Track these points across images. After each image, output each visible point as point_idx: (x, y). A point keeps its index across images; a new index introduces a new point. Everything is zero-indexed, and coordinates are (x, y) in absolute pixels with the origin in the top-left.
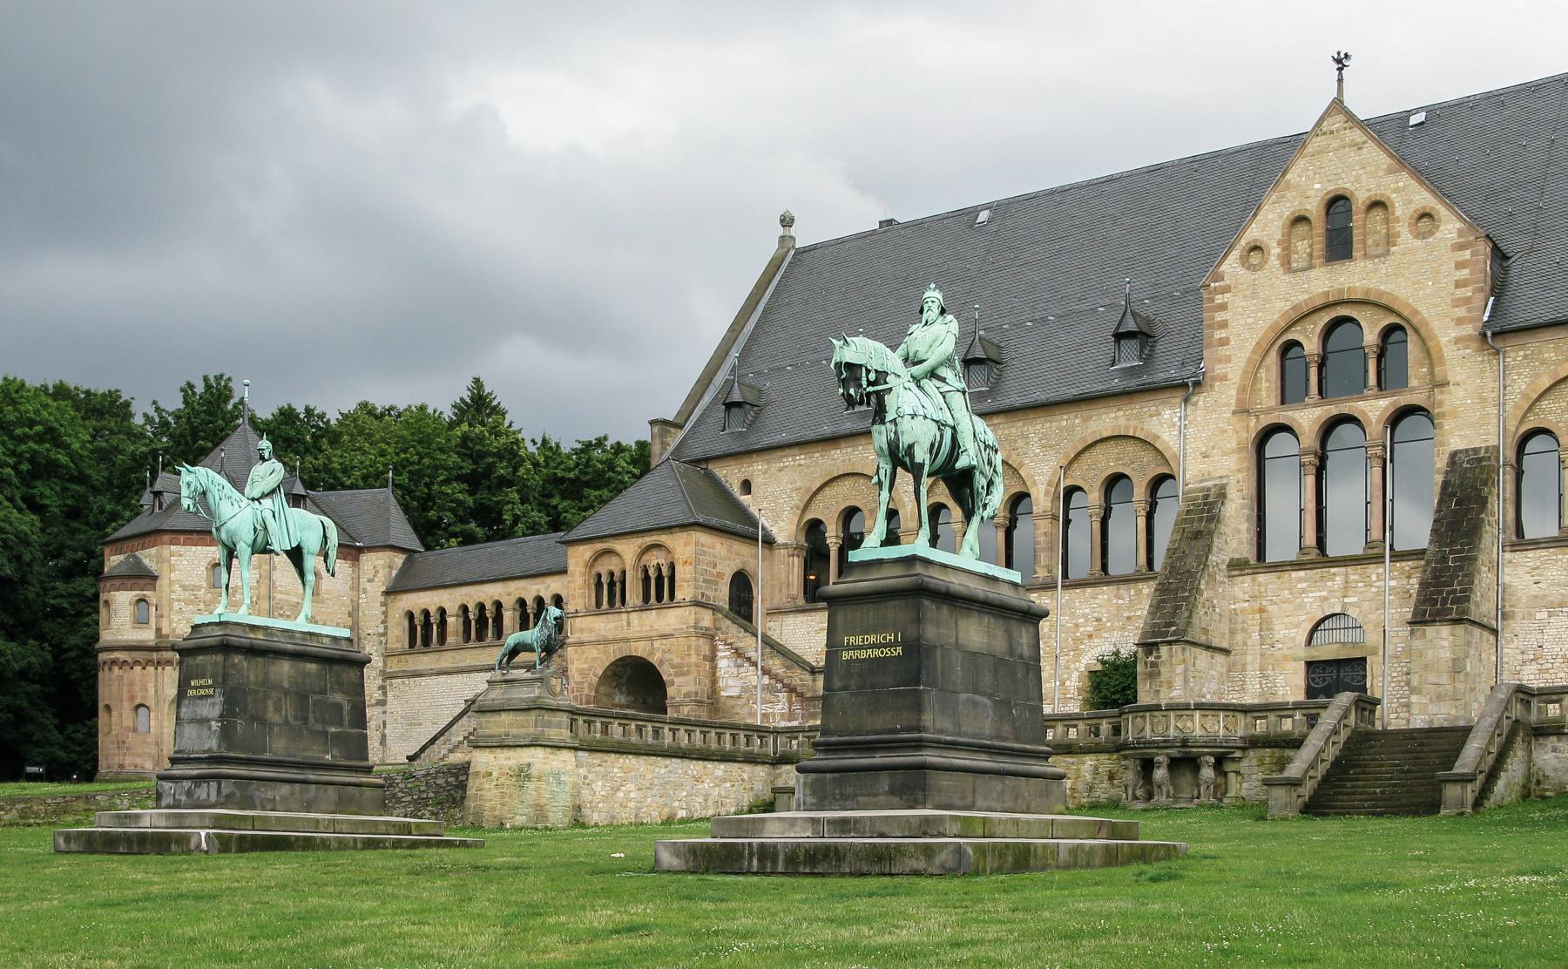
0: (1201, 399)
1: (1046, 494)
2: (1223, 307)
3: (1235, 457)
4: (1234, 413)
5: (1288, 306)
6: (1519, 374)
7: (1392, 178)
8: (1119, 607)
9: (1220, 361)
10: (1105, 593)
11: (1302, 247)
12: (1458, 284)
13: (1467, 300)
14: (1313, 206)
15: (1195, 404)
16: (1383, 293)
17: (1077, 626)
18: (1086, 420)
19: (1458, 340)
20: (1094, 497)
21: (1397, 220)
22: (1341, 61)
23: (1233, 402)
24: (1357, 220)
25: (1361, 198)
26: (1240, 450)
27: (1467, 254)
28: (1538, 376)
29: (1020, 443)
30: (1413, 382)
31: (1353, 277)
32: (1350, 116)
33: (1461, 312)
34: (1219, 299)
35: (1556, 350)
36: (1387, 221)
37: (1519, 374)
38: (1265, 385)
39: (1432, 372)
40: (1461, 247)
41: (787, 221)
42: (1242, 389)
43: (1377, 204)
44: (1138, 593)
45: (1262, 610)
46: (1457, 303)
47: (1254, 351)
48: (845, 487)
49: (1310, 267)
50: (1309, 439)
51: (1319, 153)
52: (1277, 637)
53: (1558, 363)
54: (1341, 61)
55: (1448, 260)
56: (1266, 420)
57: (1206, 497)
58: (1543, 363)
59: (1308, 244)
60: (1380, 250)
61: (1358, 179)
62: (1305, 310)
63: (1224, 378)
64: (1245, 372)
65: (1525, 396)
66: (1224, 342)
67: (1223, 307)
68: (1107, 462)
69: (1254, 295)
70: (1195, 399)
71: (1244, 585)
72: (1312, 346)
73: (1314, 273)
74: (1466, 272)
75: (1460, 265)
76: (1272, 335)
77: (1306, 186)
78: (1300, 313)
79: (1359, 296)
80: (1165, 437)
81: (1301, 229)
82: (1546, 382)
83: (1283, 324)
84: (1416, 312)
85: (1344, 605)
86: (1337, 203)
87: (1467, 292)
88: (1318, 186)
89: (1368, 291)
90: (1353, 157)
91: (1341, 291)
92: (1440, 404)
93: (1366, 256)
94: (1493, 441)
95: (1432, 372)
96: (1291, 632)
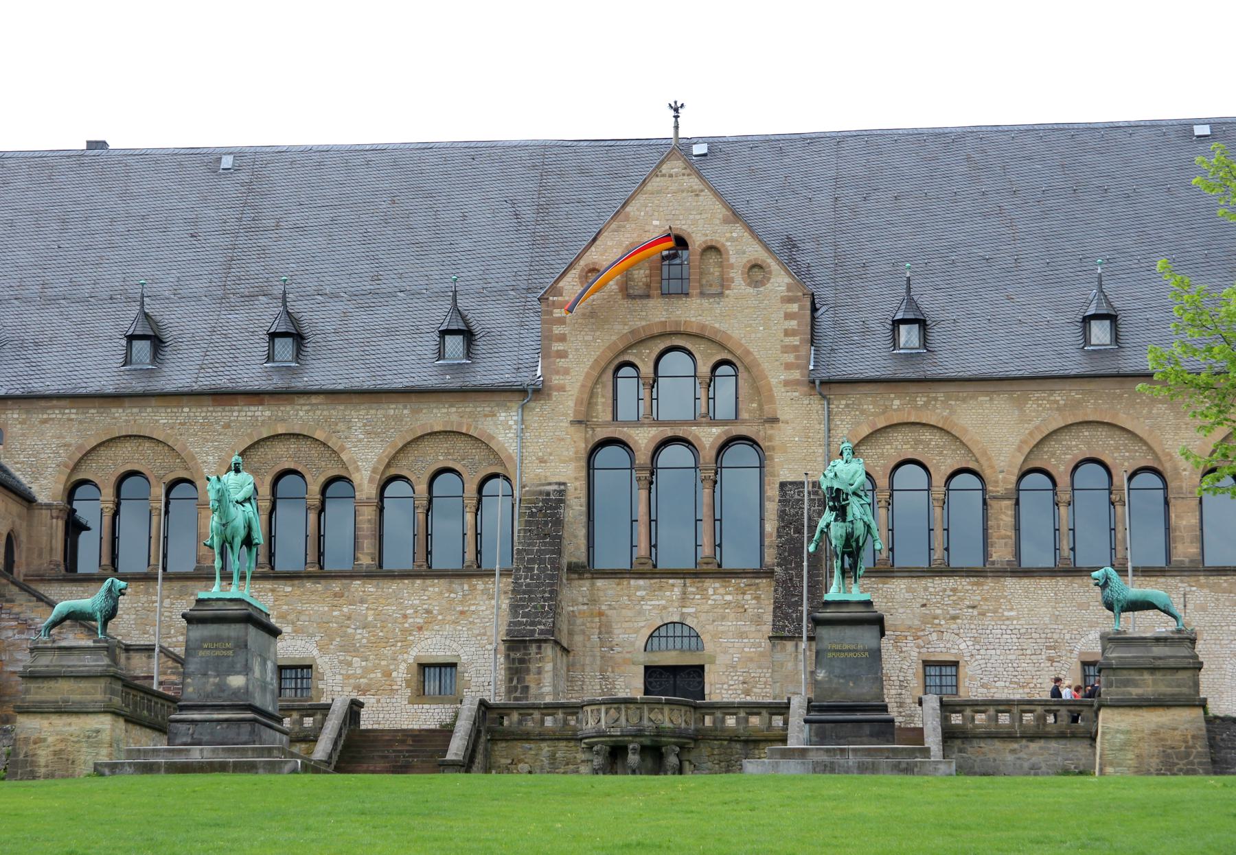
0: (538, 409)
1: (371, 480)
4: (572, 422)
5: (626, 329)
6: (842, 421)
7: (726, 227)
9: (558, 373)
12: (787, 333)
13: (795, 349)
16: (717, 331)
17: (405, 616)
18: (415, 412)
19: (787, 383)
25: (697, 240)
26: (577, 459)
27: (794, 307)
28: (858, 424)
29: (341, 426)
30: (744, 415)
33: (790, 358)
36: (721, 265)
37: (842, 421)
38: (600, 400)
39: (761, 408)
40: (790, 300)
42: (579, 402)
43: (712, 249)
44: (473, 588)
46: (786, 349)
47: (592, 368)
49: (648, 296)
51: (659, 192)
52: (616, 641)
53: (876, 415)
56: (602, 433)
58: (863, 412)
60: (713, 290)
62: (643, 336)
63: (562, 389)
64: (583, 386)
66: (562, 355)
71: (582, 588)
73: (651, 303)
75: (788, 316)
77: (650, 219)
78: (638, 338)
79: (695, 330)
82: (866, 431)
83: (621, 347)
84: (748, 352)
87: (795, 341)
88: (656, 223)
89: (703, 327)
92: (770, 439)
93: (702, 294)
95: (761, 408)
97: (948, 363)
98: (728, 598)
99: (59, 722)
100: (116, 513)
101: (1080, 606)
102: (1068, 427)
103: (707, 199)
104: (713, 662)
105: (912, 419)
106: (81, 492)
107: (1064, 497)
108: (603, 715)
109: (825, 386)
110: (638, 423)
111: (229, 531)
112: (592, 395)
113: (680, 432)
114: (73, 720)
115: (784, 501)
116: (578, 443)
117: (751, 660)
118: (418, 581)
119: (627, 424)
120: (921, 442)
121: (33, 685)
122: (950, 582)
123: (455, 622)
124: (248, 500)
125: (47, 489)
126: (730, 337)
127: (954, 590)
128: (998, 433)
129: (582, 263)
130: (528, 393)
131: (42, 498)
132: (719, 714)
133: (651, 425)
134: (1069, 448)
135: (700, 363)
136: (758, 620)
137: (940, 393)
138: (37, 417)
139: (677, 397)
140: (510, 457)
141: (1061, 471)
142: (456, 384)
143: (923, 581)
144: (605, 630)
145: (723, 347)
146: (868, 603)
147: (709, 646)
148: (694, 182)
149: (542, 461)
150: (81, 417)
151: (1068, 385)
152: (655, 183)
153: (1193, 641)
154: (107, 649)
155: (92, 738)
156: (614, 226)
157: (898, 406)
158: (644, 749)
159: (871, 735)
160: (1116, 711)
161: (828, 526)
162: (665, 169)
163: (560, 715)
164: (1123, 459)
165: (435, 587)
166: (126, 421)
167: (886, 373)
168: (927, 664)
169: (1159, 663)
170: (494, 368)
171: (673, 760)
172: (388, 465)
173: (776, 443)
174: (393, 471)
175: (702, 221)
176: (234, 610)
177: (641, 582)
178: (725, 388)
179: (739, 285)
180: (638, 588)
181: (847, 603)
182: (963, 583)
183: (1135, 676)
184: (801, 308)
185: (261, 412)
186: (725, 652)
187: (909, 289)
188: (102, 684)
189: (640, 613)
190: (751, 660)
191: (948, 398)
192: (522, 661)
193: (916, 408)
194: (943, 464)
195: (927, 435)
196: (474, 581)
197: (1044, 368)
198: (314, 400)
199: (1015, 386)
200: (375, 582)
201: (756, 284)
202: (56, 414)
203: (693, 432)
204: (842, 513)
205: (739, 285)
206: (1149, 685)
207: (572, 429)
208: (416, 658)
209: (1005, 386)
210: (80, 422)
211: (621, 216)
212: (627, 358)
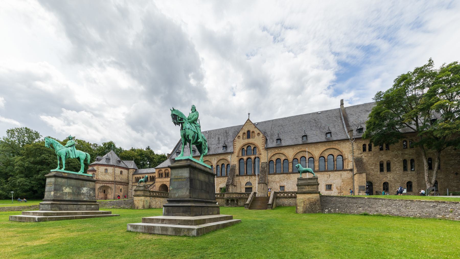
0: (233, 155)
10: (222, 178)
11: (245, 136)
14: (246, 132)
20: (220, 166)
22: (249, 114)
24: (251, 133)
25: (251, 131)
31: (250, 141)
32: (250, 121)
43: (253, 132)
50: (245, 160)
54: (249, 114)
56: (240, 158)
59: (245, 136)
72: (245, 149)
86: (249, 131)
96: (243, 184)
97: (283, 144)
113: (250, 157)
115: (262, 165)
122: (283, 175)
130: (232, 153)
141: (299, 158)
144: (240, 183)
157: (277, 151)
168: (280, 186)
170: (229, 150)
175: (252, 129)
179: (256, 136)
182: (285, 175)
194: (283, 158)
201: (258, 136)
205: (256, 136)
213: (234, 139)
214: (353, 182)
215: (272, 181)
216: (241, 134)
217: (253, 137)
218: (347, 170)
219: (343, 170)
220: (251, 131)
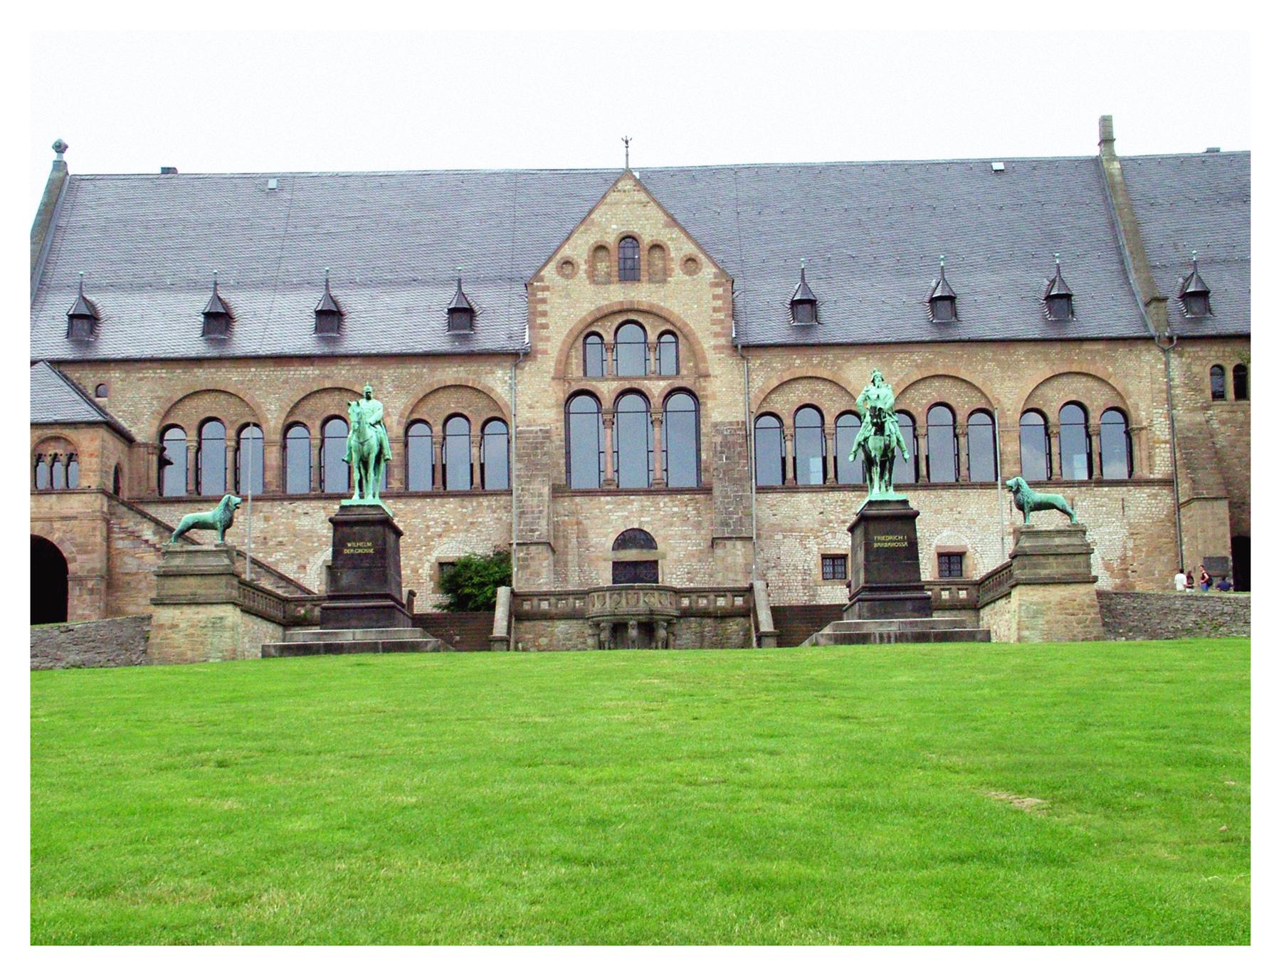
0: (529, 367)
1: (399, 423)
2: (544, 301)
3: (555, 410)
4: (553, 378)
8: (464, 515)
9: (541, 340)
12: (715, 310)
13: (721, 322)
14: (611, 239)
15: (523, 368)
16: (662, 308)
17: (428, 527)
19: (716, 347)
21: (672, 259)
23: (552, 370)
24: (644, 254)
25: (646, 240)
27: (720, 291)
30: (684, 372)
31: (642, 294)
33: (717, 329)
34: (540, 295)
35: (782, 362)
36: (664, 259)
38: (574, 361)
39: (696, 366)
40: (716, 285)
41: (60, 148)
42: (558, 362)
43: (656, 247)
44: (480, 504)
45: (579, 523)
46: (714, 322)
47: (568, 336)
48: (207, 399)
49: (610, 283)
52: (593, 543)
53: (784, 371)
55: (707, 294)
56: (575, 387)
57: (535, 438)
58: (773, 369)
61: (643, 227)
63: (545, 352)
65: (761, 390)
66: (545, 326)
67: (544, 301)
68: (450, 403)
69: (568, 296)
70: (522, 365)
73: (612, 287)
74: (720, 302)
75: (716, 297)
76: (581, 327)
78: (602, 314)
79: (645, 307)
80: (499, 390)
81: (602, 254)
82: (775, 383)
85: (641, 523)
87: (721, 316)
88: (614, 227)
89: (652, 305)
90: (640, 210)
91: (632, 302)
92: (704, 389)
93: (650, 281)
94: (741, 418)
95: (696, 366)
98: (675, 509)
99: (189, 612)
100: (199, 449)
101: (936, 512)
102: (924, 379)
103: (653, 210)
104: (664, 557)
105: (810, 374)
106: (170, 434)
107: (921, 431)
108: (608, 599)
109: (744, 349)
110: (603, 378)
111: (365, 448)
112: (568, 357)
113: (635, 385)
114: (201, 609)
116: (558, 393)
117: (693, 556)
118: (437, 500)
119: (594, 379)
120: (816, 391)
121: (169, 583)
123: (467, 531)
124: (379, 422)
125: (144, 431)
126: (671, 313)
127: (843, 501)
128: (874, 384)
129: (558, 257)
130: (517, 357)
131: (139, 438)
132: (694, 597)
133: (614, 380)
134: (925, 395)
135: (649, 332)
136: (698, 525)
137: (830, 355)
138: (135, 376)
139: (629, 361)
140: (506, 404)
141: (919, 412)
142: (464, 349)
143: (820, 495)
144: (582, 535)
145: (666, 320)
146: (905, 502)
147: (661, 546)
148: (642, 196)
149: (531, 407)
150: (169, 375)
151: (923, 349)
152: (613, 196)
153: (1084, 532)
154: (227, 552)
155: (217, 624)
156: (582, 228)
157: (799, 364)
158: (641, 625)
159: (914, 610)
160: (1029, 587)
161: (866, 440)
162: (620, 186)
163: (712, 597)
164: (964, 402)
165: (451, 504)
166: (206, 379)
167: (791, 340)
168: (824, 557)
169: (1061, 550)
171: (662, 633)
172: (412, 412)
173: (709, 392)
174: (416, 416)
175: (650, 227)
176: (372, 515)
177: (609, 498)
178: (668, 352)
179: (678, 275)
180: (608, 503)
181: (888, 502)
183: (1042, 560)
184: (725, 291)
185: (311, 371)
186: (673, 550)
187: (803, 278)
188: (224, 580)
189: (608, 522)
190: (693, 556)
191: (836, 358)
192: (525, 559)
193: (814, 366)
195: (820, 386)
196: (481, 499)
197: (905, 336)
198: (353, 362)
199: (885, 350)
200: (404, 500)
202: (150, 373)
203: (646, 385)
204: (880, 429)
205: (678, 275)
206: (1054, 568)
207: (553, 383)
208: (437, 558)
209: (878, 350)
210: (170, 380)
211: (588, 221)
212: (594, 329)
213: (537, 276)
214: (1178, 542)
215: (776, 528)
216: (578, 249)
217: (662, 277)
218: (1149, 483)
219: (1132, 480)
220: (646, 240)
